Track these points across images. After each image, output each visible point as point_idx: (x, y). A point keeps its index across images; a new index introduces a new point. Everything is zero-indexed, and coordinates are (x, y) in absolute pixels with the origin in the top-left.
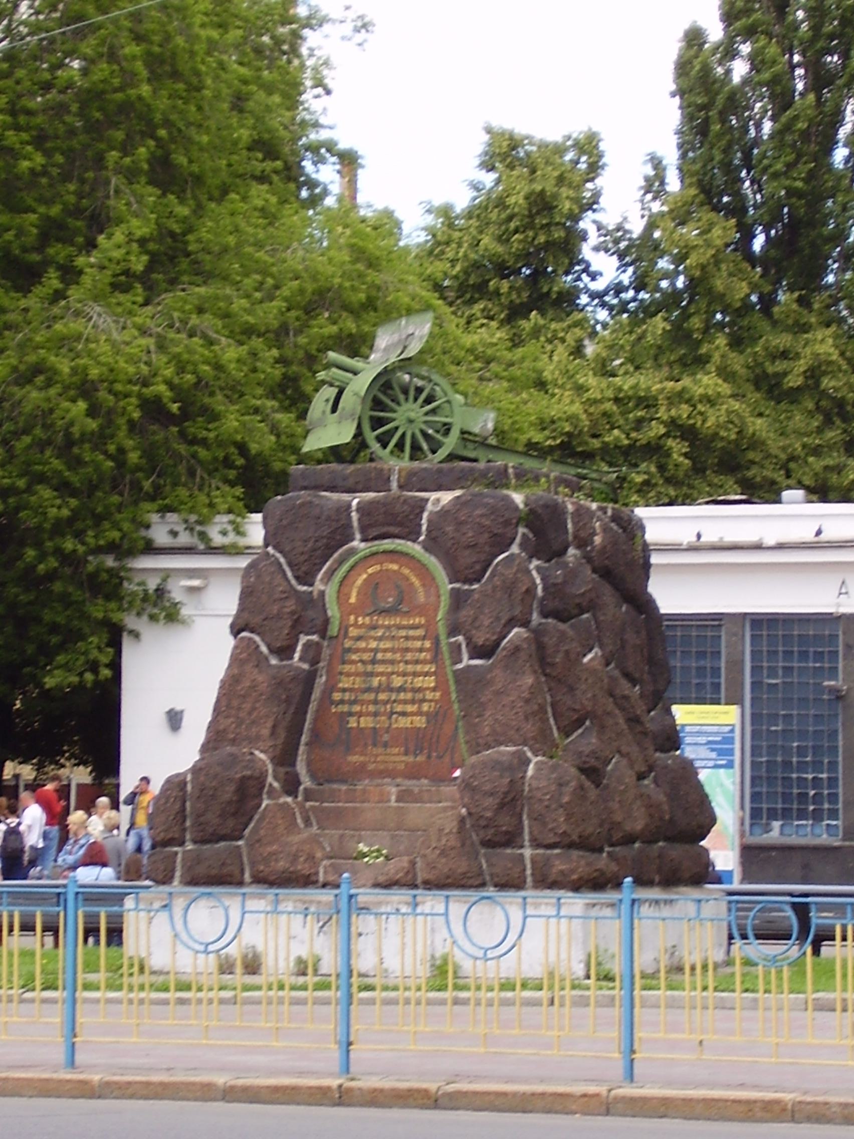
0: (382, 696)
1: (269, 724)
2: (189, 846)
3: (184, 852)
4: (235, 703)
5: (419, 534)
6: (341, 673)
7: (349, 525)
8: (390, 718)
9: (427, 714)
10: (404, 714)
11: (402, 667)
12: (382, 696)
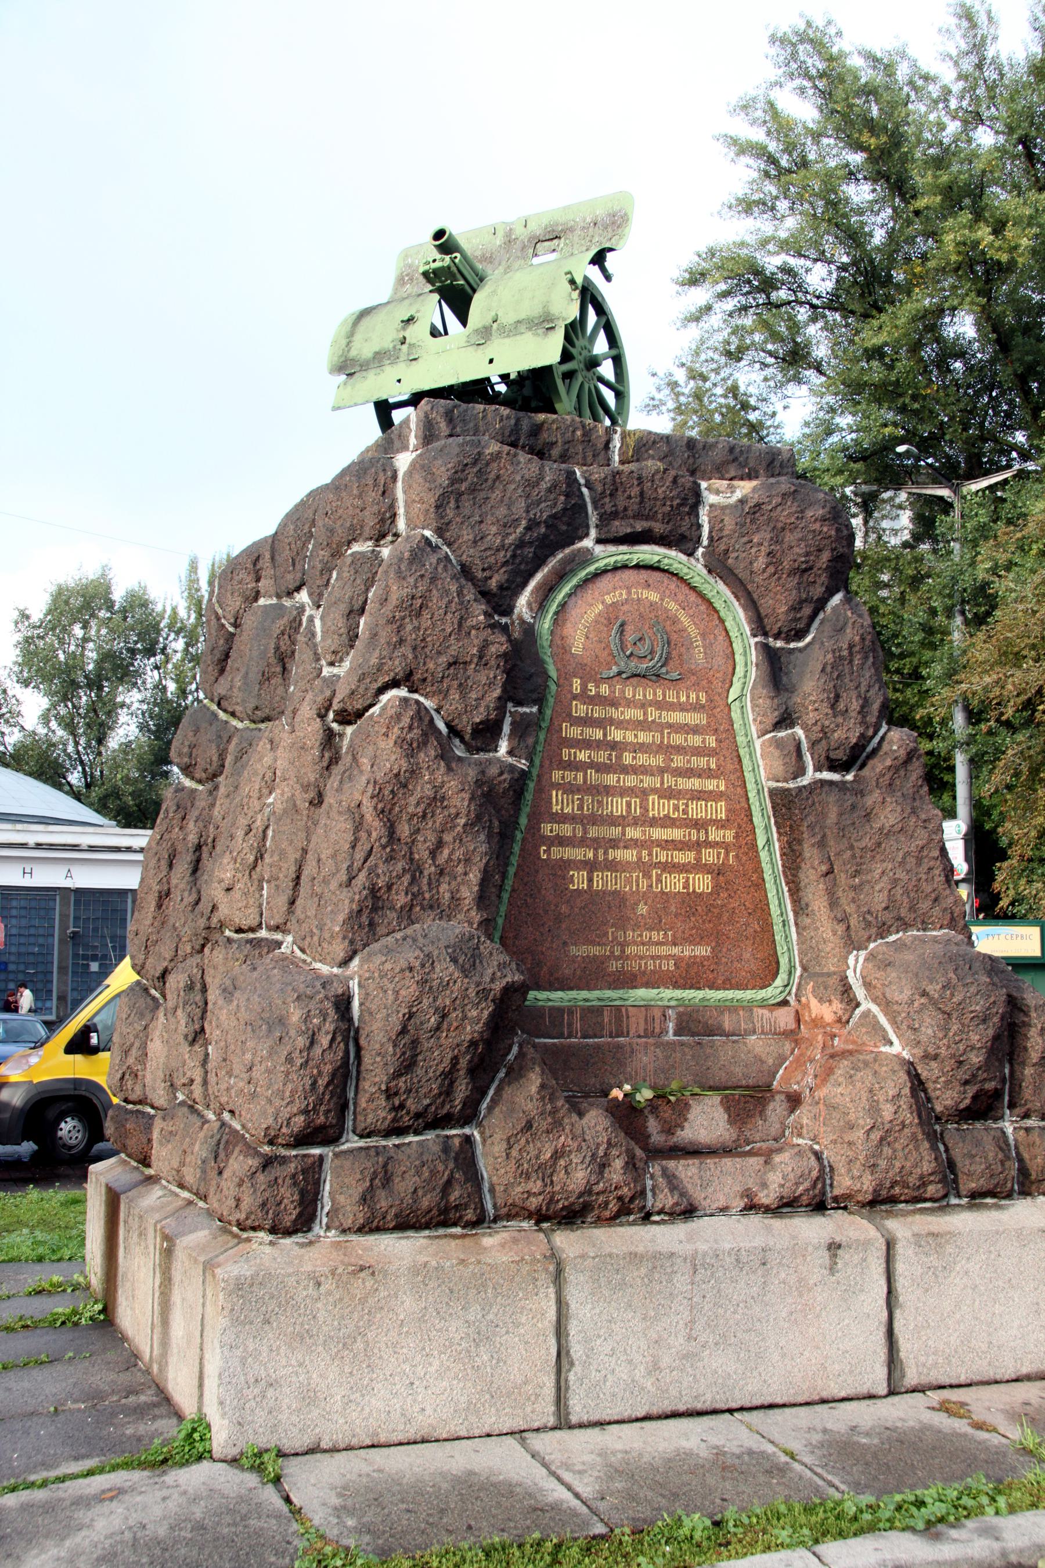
0: (633, 833)
1: (474, 877)
4: (404, 830)
6: (558, 786)
8: (647, 875)
9: (717, 872)
10: (670, 867)
11: (669, 780)
12: (633, 833)
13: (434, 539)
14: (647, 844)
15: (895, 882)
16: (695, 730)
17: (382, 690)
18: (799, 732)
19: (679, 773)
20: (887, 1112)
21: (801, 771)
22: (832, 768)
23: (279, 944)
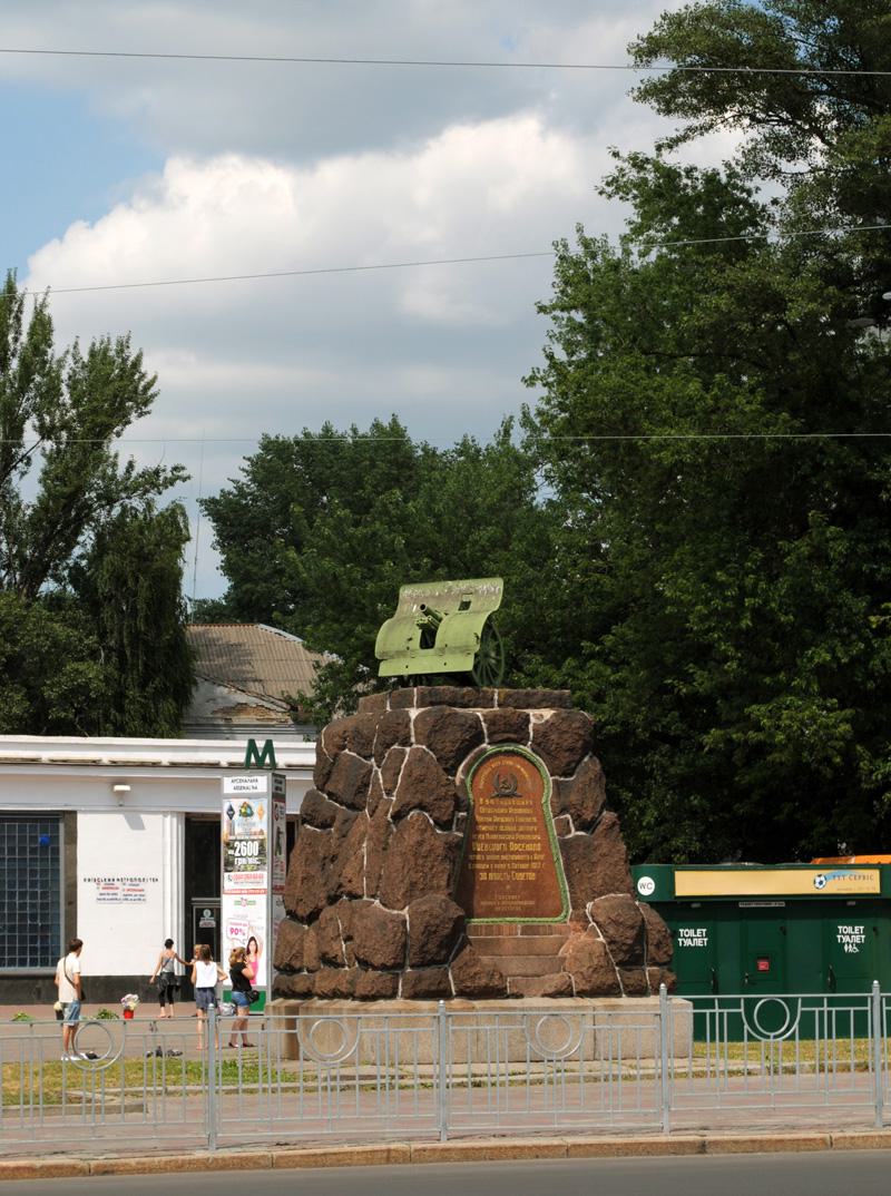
0: (504, 857)
1: (445, 877)
7: (482, 732)
9: (537, 871)
11: (519, 837)
12: (504, 857)
13: (427, 750)
14: (510, 862)
15: (606, 874)
16: (528, 815)
17: (411, 810)
18: (568, 816)
19: (521, 833)
20: (596, 961)
21: (569, 832)
22: (582, 830)
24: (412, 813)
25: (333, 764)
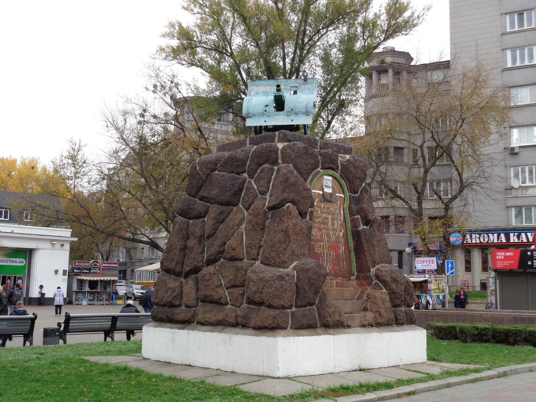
2: (294, 309)
3: (293, 313)
5: (338, 169)
17: (286, 203)
18: (359, 216)
23: (255, 264)
24: (287, 205)
25: (205, 181)
